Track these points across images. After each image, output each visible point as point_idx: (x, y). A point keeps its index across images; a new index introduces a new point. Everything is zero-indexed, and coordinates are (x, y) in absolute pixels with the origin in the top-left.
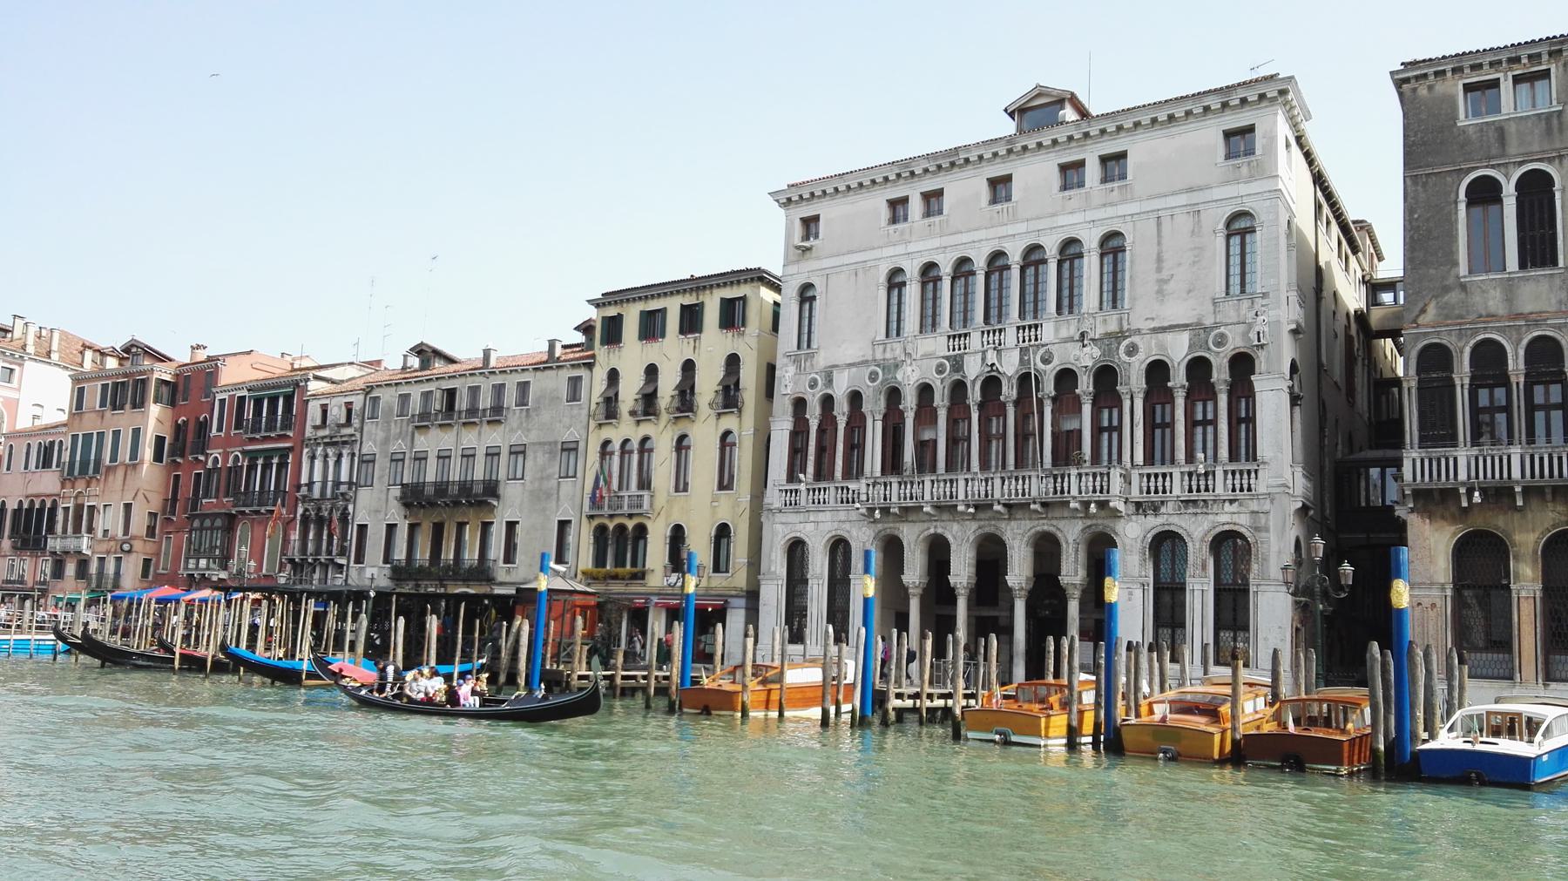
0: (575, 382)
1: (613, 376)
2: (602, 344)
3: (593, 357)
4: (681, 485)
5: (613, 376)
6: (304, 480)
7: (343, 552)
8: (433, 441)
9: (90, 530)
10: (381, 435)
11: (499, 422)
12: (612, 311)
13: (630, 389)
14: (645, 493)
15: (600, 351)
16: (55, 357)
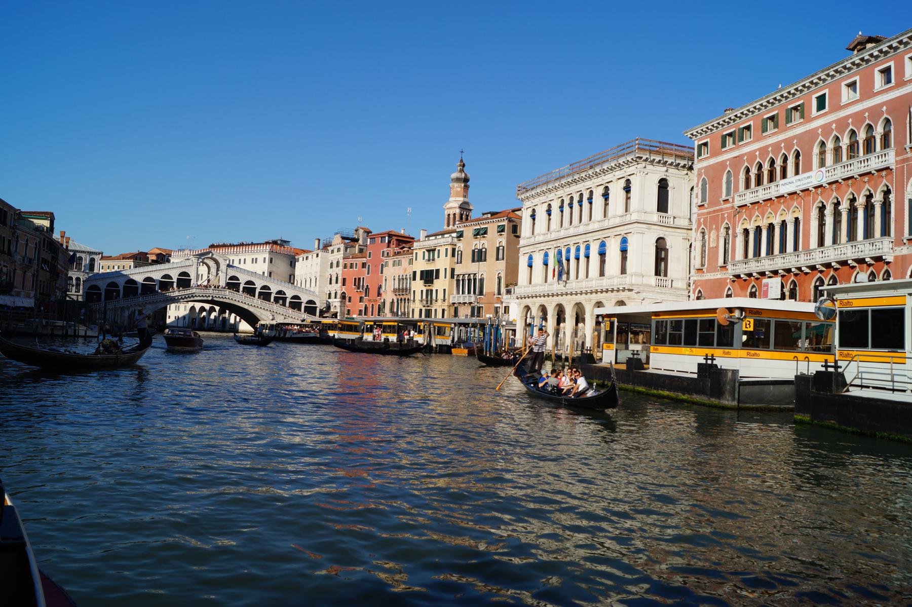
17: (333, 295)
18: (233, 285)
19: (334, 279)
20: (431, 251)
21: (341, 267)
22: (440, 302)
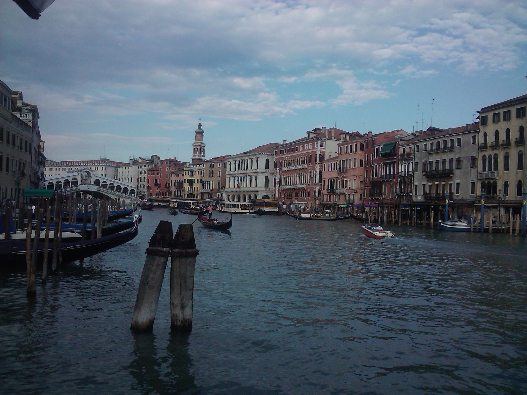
0: (474, 137)
1: (485, 135)
2: (482, 125)
3: (479, 129)
4: (506, 168)
5: (485, 135)
6: (400, 171)
7: (411, 191)
8: (434, 158)
9: (346, 187)
10: (419, 156)
11: (452, 151)
12: (484, 115)
13: (491, 139)
14: (496, 172)
15: (481, 128)
16: (333, 138)
17: (142, 187)
18: (97, 182)
19: (143, 179)
20: (192, 171)
21: (146, 174)
22: (196, 192)
